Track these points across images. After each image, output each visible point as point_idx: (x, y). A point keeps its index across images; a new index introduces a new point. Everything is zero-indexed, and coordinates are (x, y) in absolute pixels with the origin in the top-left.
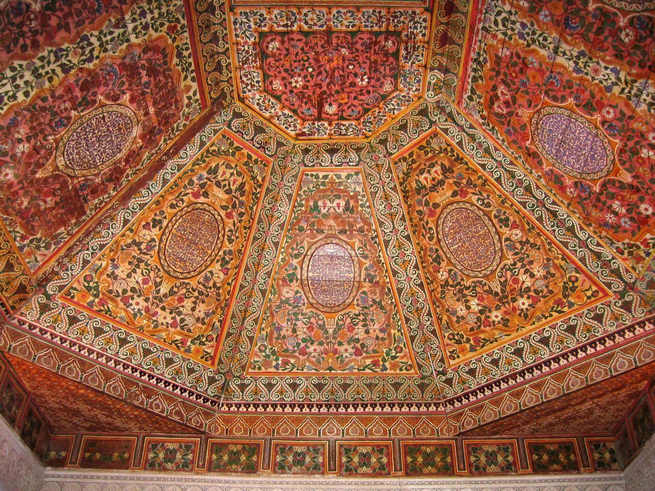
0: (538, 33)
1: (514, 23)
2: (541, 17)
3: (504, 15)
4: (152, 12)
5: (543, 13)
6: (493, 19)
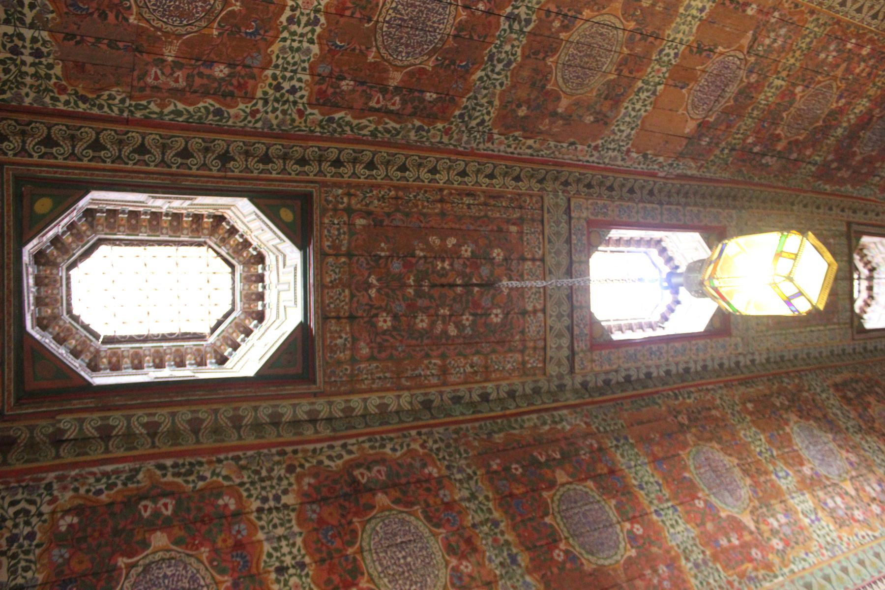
0: (31, 557)
1: (27, 523)
2: (56, 552)
3: (33, 509)
4: (33, 65)
5: (63, 551)
6: (19, 497)
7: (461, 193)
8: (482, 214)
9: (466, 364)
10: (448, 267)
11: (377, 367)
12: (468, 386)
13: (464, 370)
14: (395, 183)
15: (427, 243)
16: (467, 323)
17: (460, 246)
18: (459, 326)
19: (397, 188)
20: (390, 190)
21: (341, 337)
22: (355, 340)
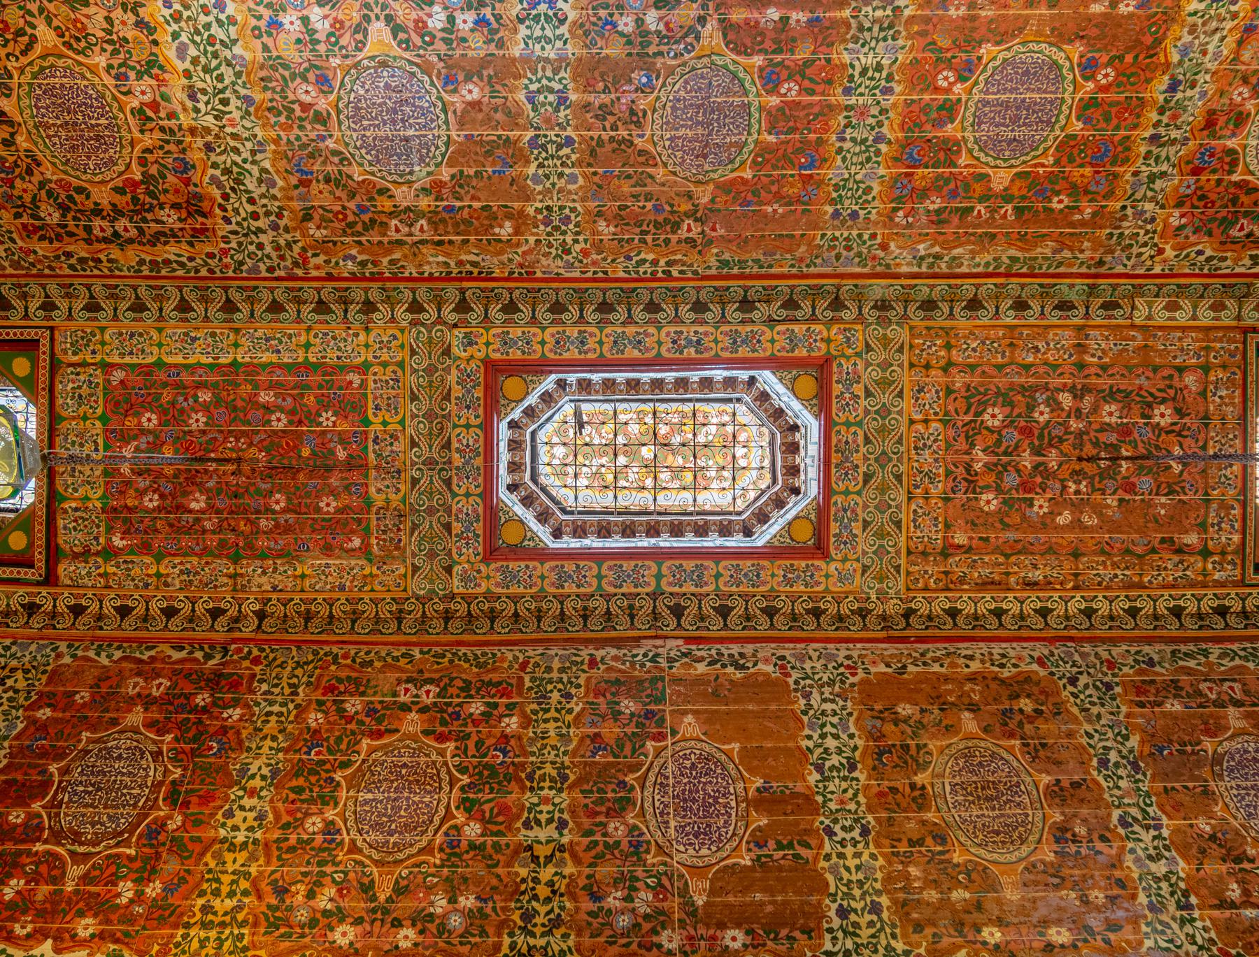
7: (1048, 584)
8: (1013, 559)
9: (1045, 353)
10: (1070, 484)
11: (1175, 357)
12: (1044, 322)
13: (1048, 344)
14: (1144, 593)
15: (1100, 515)
16: (1042, 407)
17: (1051, 513)
18: (1055, 406)
19: (1141, 586)
20: (1150, 582)
21: (1220, 397)
22: (1203, 394)
